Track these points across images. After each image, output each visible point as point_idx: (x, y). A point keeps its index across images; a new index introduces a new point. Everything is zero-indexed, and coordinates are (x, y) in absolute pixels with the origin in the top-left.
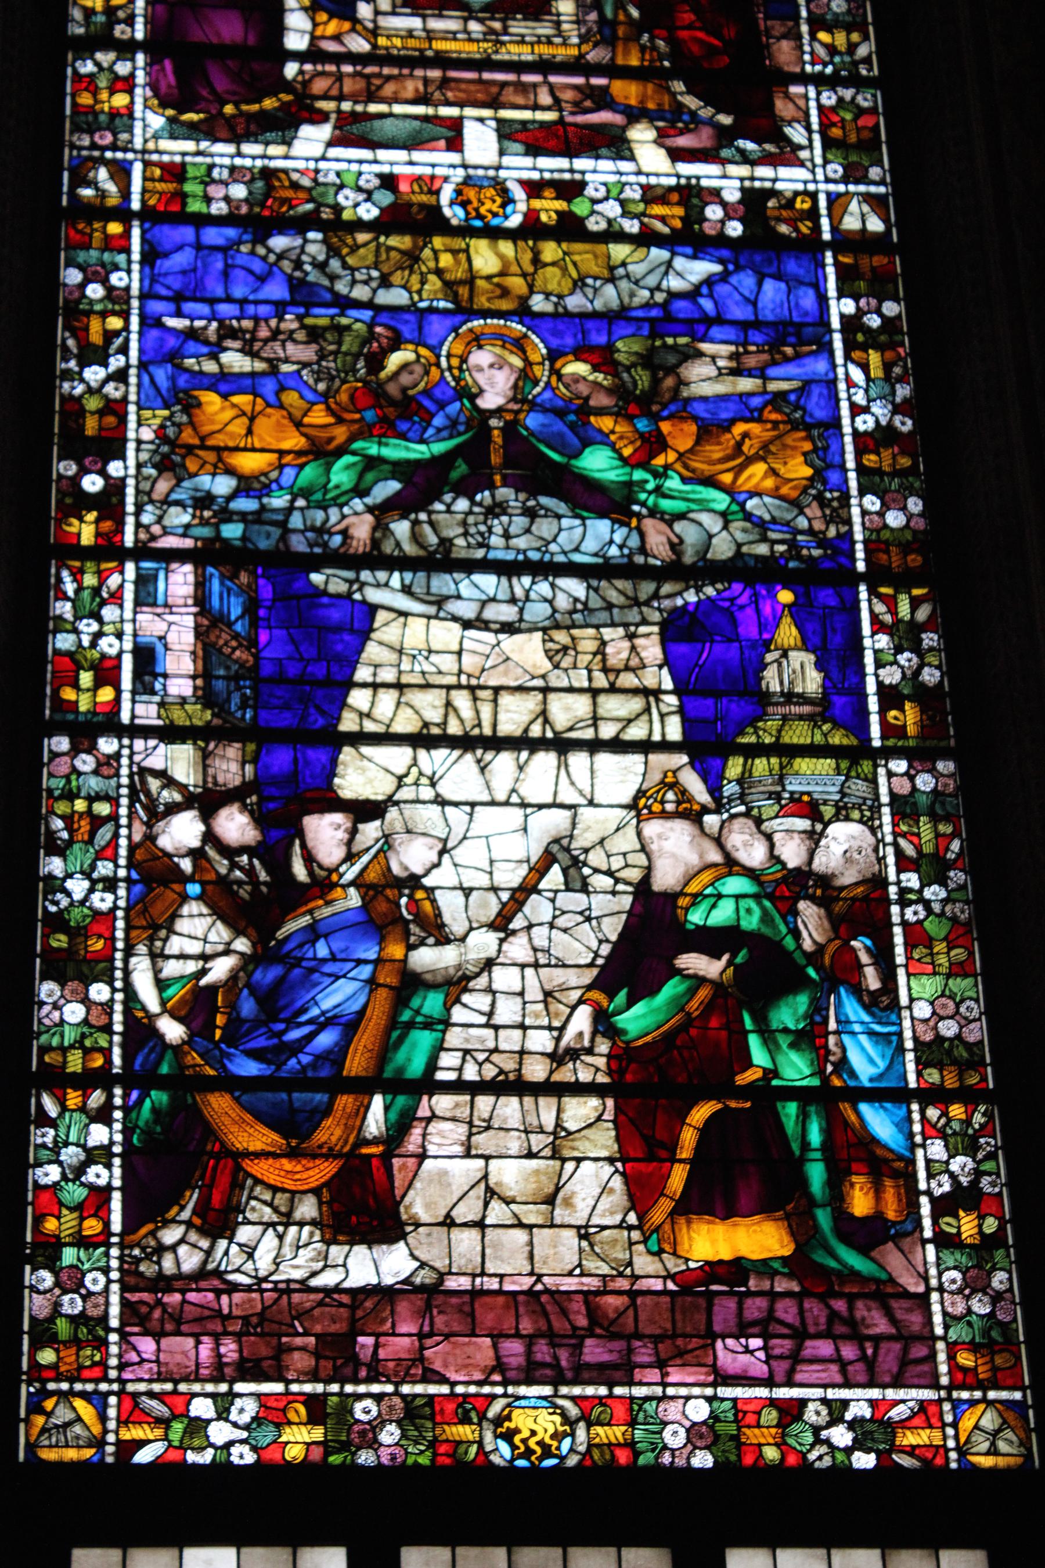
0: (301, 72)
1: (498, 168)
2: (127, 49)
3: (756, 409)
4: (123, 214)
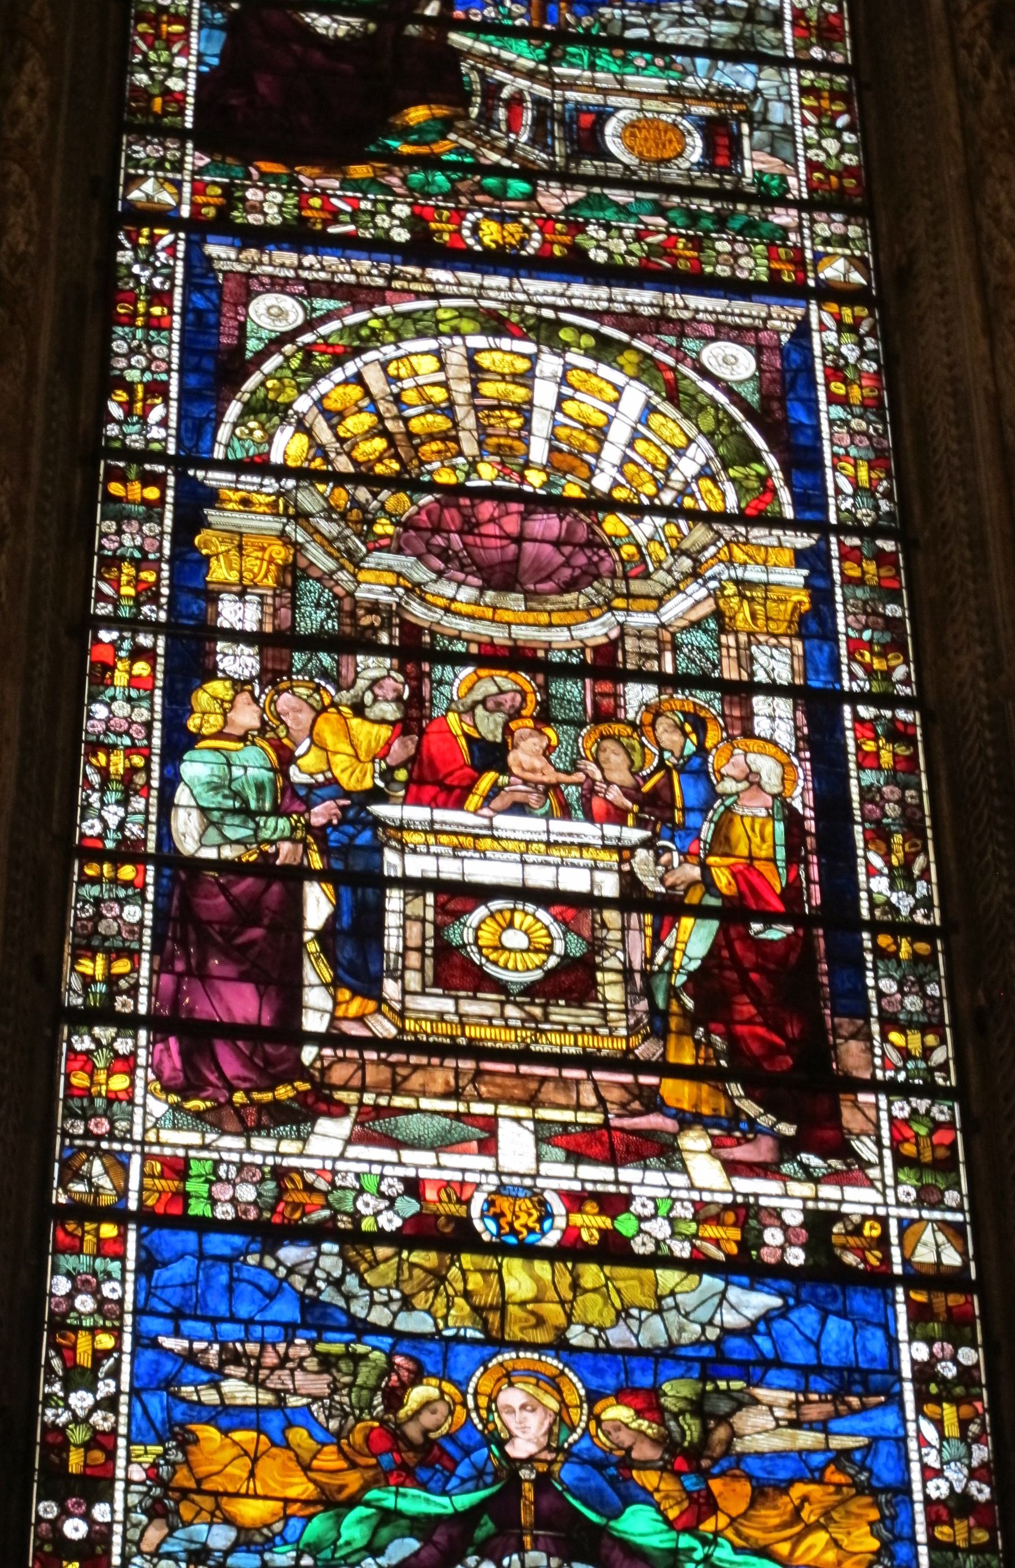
0: (320, 1057)
1: (535, 1176)
2: (129, 1023)
3: (817, 1469)
4: (119, 1215)
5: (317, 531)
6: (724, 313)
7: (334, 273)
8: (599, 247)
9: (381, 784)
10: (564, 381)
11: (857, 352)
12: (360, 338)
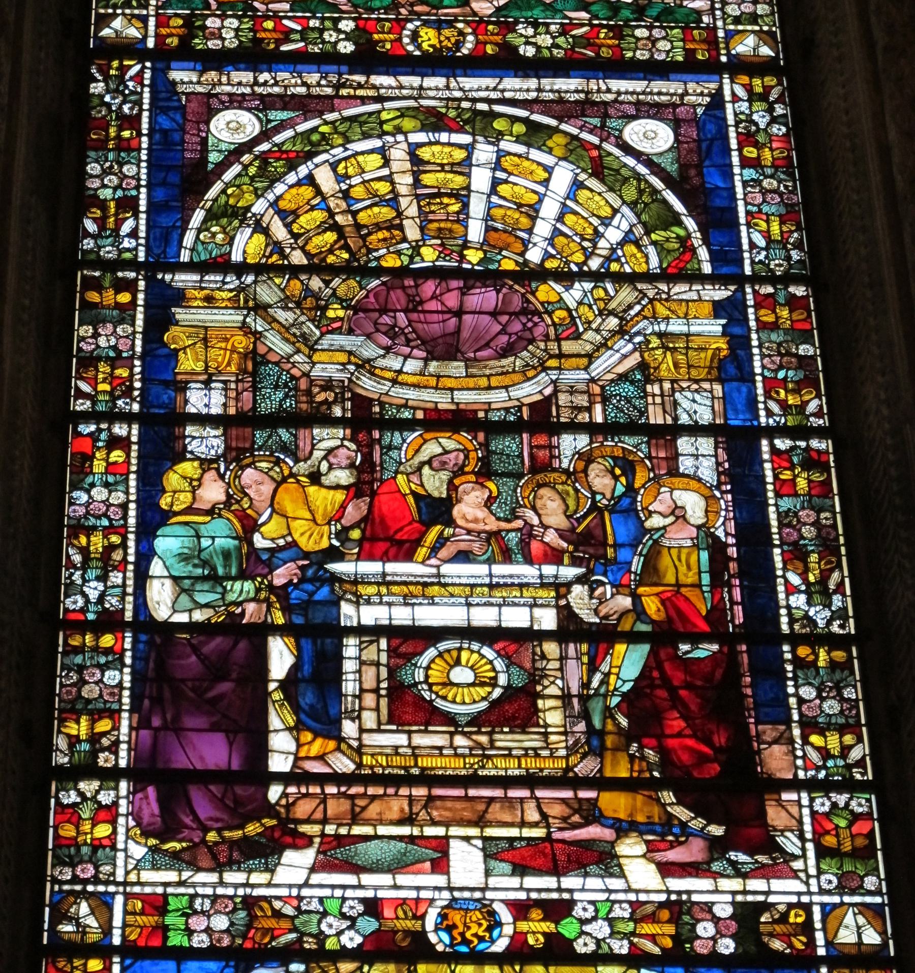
0: (285, 795)
2: (111, 776)
5: (275, 320)
6: (644, 93)
7: (286, 87)
8: (527, 43)
9: (336, 543)
10: (497, 166)
11: (768, 118)
12: (311, 143)
